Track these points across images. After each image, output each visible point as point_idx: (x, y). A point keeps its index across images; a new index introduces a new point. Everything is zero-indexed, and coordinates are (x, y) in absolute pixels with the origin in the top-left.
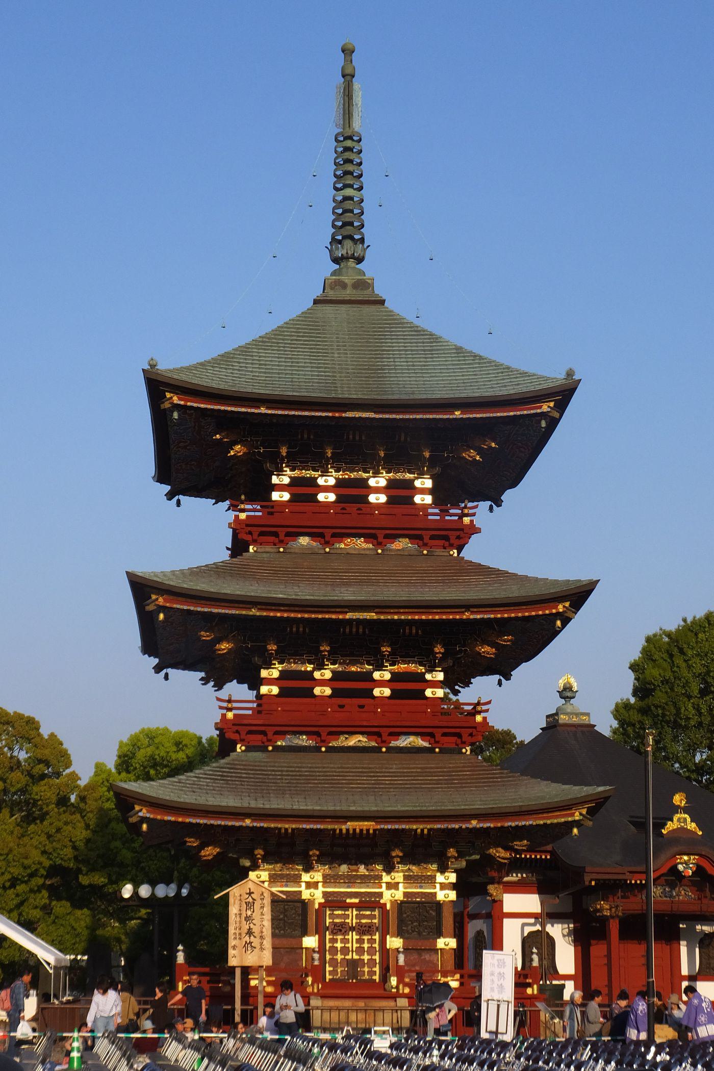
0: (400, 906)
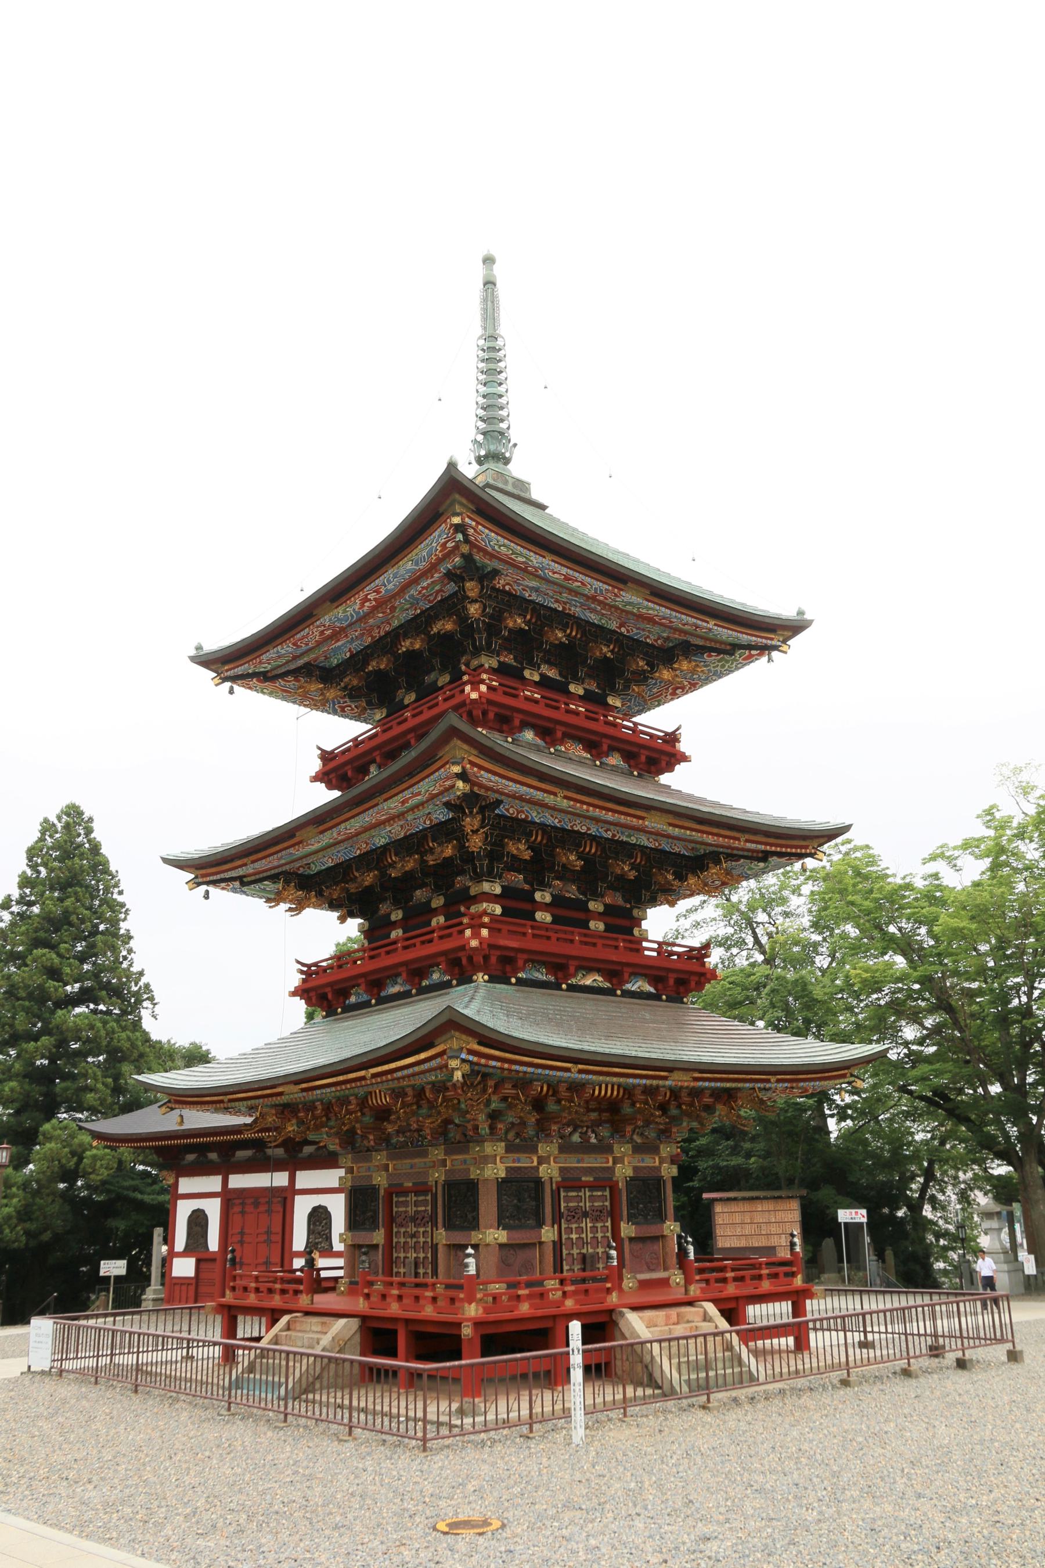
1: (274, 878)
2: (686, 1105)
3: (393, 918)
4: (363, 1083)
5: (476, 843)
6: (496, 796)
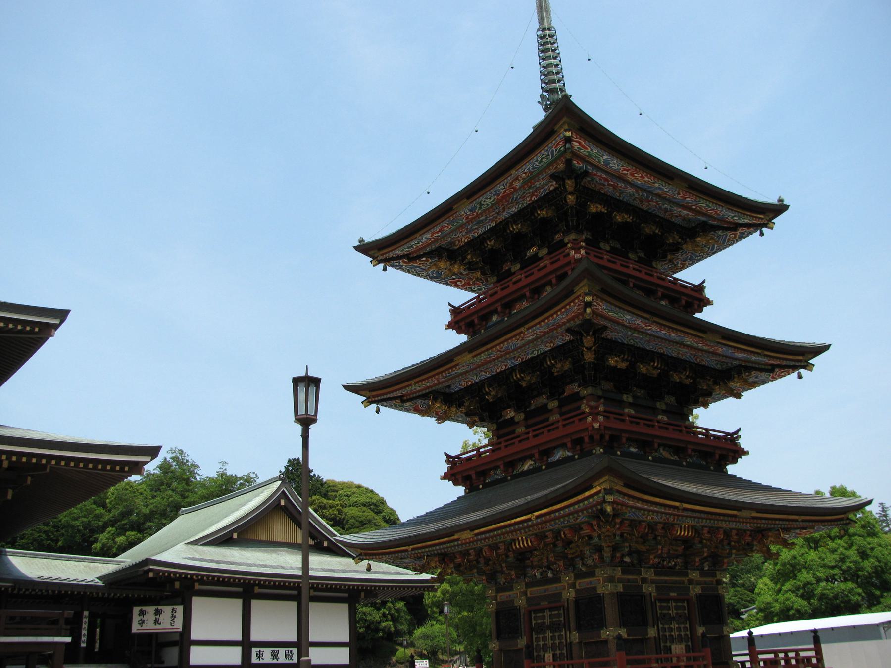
0: (699, 597)
1: (424, 396)
2: (735, 542)
3: (516, 419)
4: (530, 523)
5: (589, 357)
6: (603, 322)
